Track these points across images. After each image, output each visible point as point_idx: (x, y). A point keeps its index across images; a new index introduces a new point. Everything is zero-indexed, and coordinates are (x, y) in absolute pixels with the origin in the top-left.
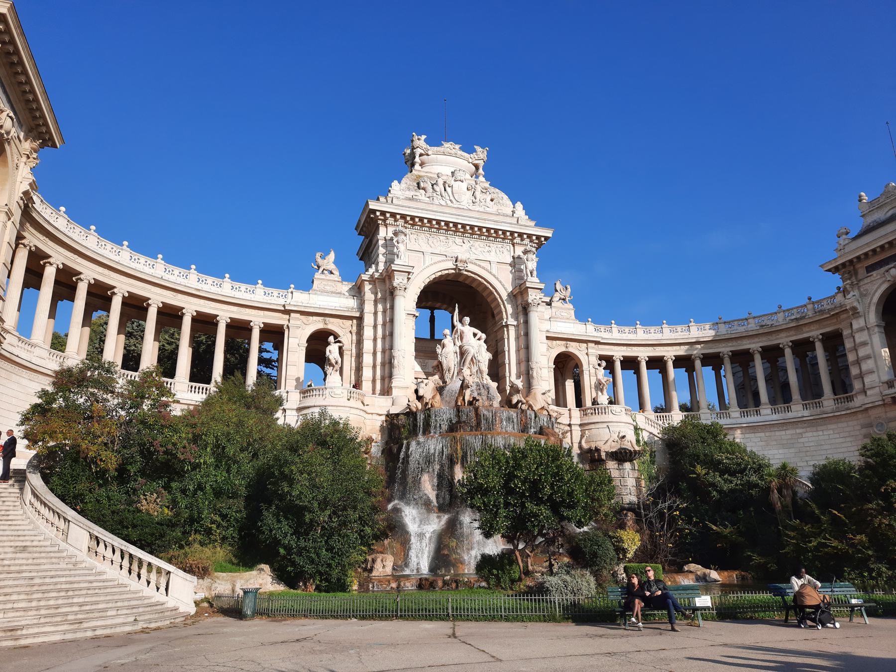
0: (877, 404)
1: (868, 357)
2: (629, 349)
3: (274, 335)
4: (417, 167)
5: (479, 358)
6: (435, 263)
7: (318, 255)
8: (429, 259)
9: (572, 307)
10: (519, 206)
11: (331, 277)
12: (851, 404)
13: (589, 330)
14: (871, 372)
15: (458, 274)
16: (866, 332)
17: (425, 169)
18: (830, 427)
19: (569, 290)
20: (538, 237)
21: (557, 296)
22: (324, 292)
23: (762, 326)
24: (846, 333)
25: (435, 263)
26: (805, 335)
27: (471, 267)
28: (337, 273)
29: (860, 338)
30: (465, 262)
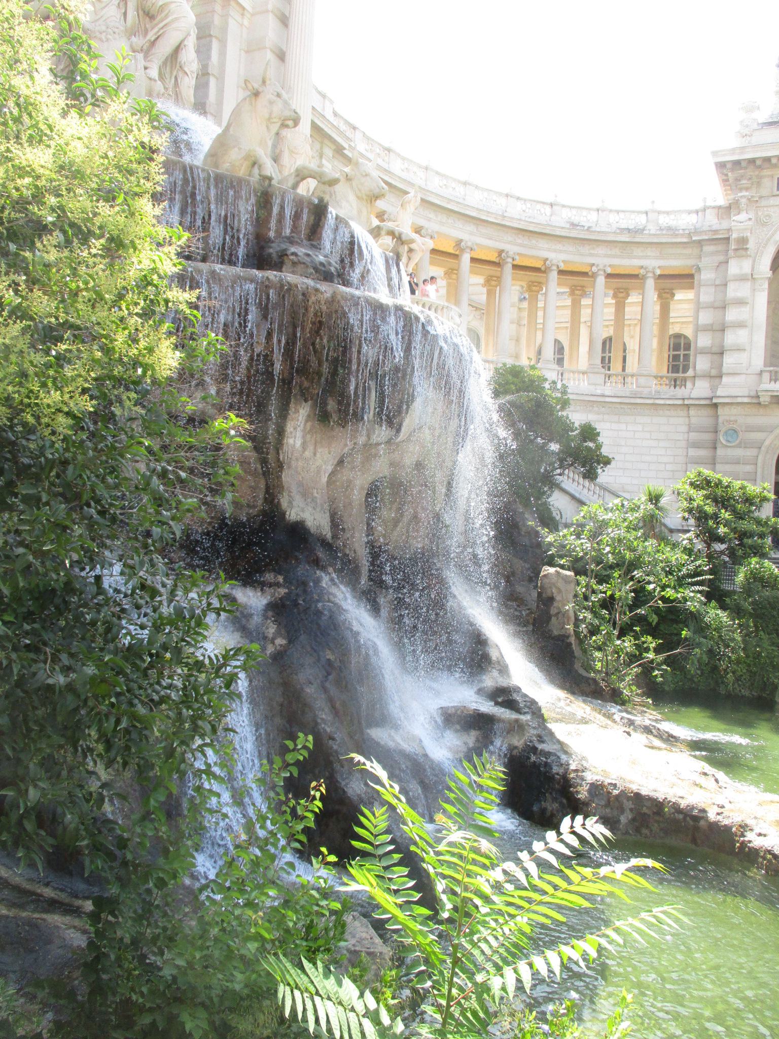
0: (739, 400)
1: (741, 325)
12: (680, 392)
14: (739, 349)
16: (748, 284)
18: (640, 419)
23: (573, 224)
24: (706, 276)
26: (637, 262)
29: (734, 291)
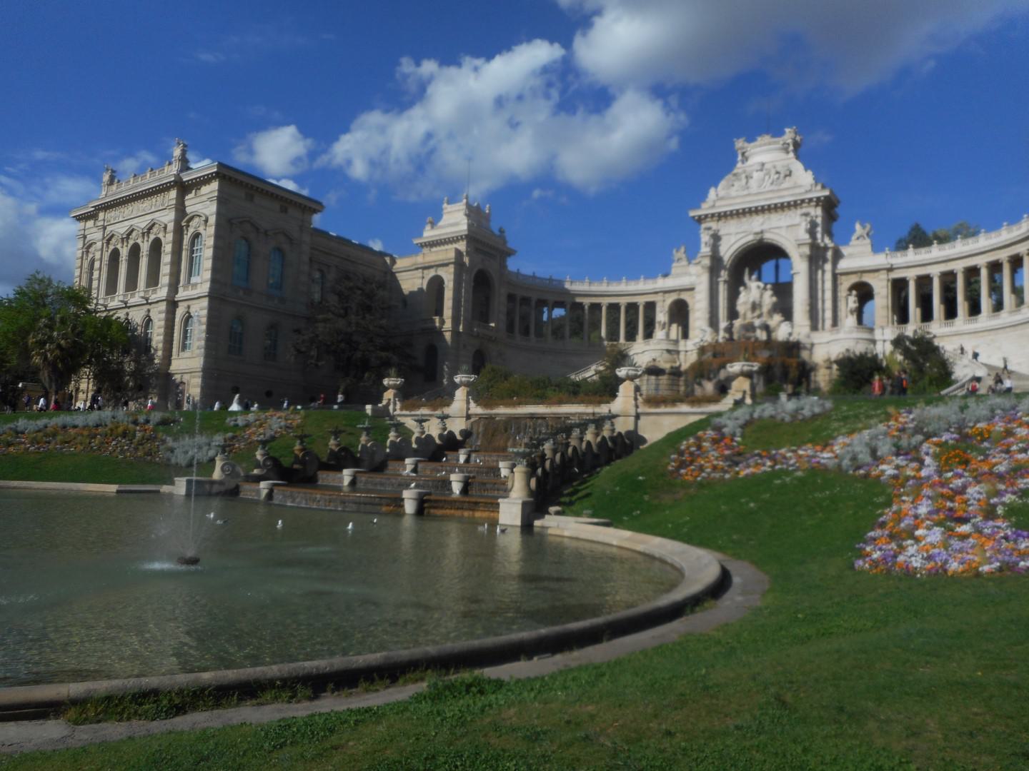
2: (923, 268)
3: (651, 307)
4: (739, 165)
6: (738, 240)
7: (674, 251)
13: (881, 260)
15: (761, 241)
17: (750, 162)
19: (868, 226)
20: (818, 198)
21: (854, 238)
22: (678, 275)
25: (738, 240)
30: (756, 234)
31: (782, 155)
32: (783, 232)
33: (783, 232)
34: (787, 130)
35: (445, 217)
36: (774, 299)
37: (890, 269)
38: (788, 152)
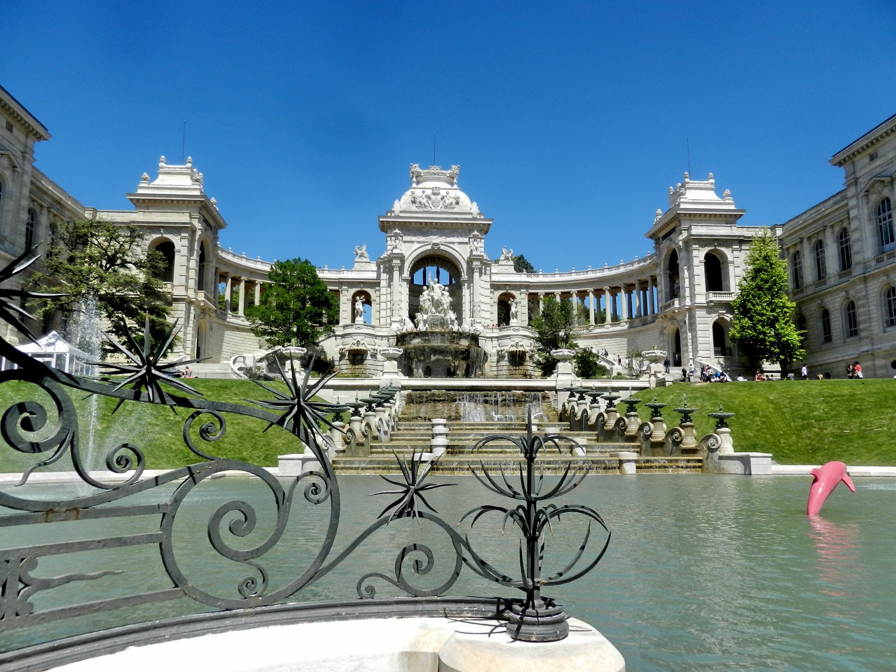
4: (414, 185)
5: (444, 301)
8: (416, 246)
9: (512, 263)
10: (475, 204)
11: (364, 260)
13: (523, 278)
21: (502, 258)
27: (442, 247)
28: (366, 255)
30: (436, 244)
31: (449, 186)
32: (456, 247)
33: (456, 247)
34: (454, 166)
35: (161, 176)
36: (450, 299)
37: (527, 286)
38: (452, 184)
